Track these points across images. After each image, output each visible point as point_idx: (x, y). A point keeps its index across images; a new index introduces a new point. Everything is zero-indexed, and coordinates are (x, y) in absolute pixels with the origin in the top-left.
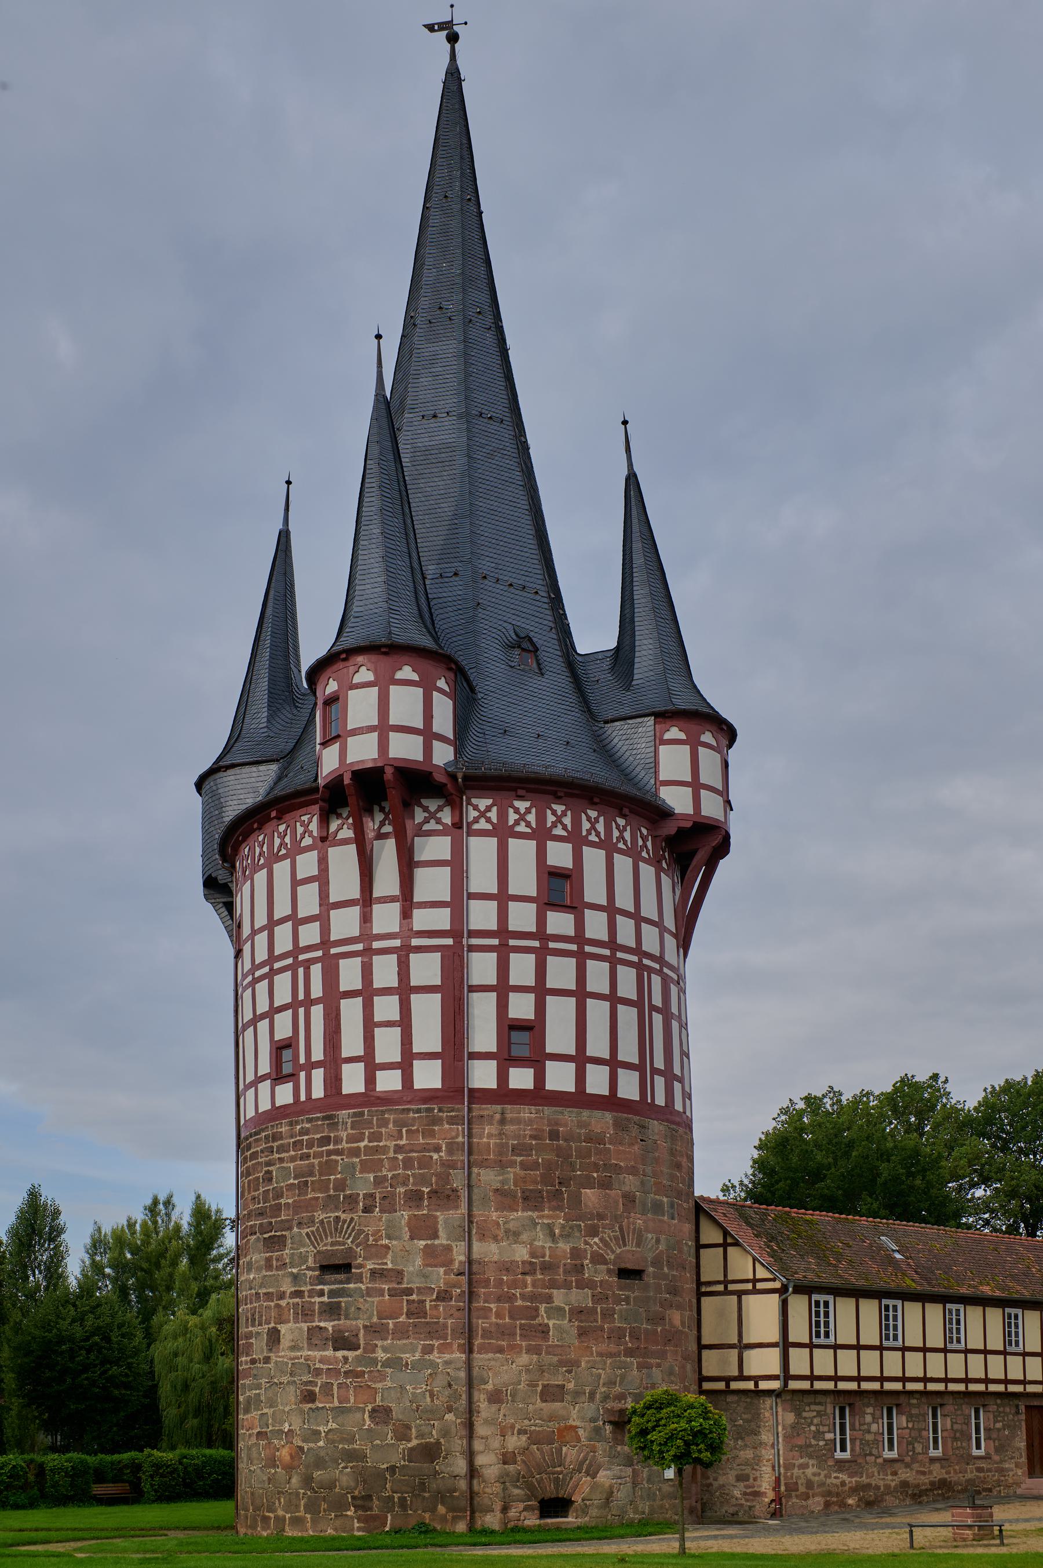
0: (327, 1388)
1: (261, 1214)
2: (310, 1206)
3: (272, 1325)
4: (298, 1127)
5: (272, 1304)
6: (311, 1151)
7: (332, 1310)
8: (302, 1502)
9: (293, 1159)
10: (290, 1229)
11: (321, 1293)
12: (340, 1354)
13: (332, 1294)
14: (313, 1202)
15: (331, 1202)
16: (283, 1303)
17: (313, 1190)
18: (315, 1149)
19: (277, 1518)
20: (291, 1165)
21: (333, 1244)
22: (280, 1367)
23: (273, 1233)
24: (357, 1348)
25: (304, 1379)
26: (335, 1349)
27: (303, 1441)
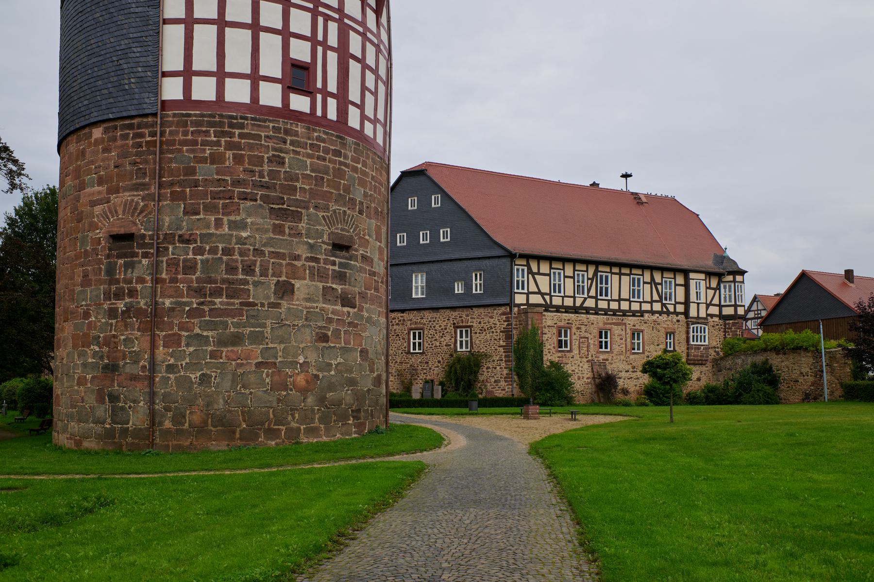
0: (337, 332)
1: (268, 188)
2: (326, 196)
3: (283, 278)
4: (316, 134)
5: (284, 262)
6: (328, 157)
7: (341, 277)
8: (317, 416)
9: (309, 156)
10: (307, 208)
11: (334, 263)
12: (346, 309)
13: (341, 265)
14: (328, 195)
15: (340, 199)
16: (296, 263)
17: (328, 186)
18: (330, 156)
19: (289, 430)
20: (309, 161)
21: (342, 230)
22: (294, 313)
23: (285, 206)
24: (354, 307)
25: (319, 324)
26: (343, 306)
27: (318, 370)
